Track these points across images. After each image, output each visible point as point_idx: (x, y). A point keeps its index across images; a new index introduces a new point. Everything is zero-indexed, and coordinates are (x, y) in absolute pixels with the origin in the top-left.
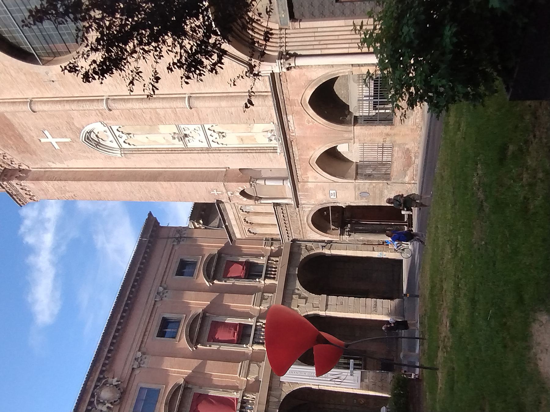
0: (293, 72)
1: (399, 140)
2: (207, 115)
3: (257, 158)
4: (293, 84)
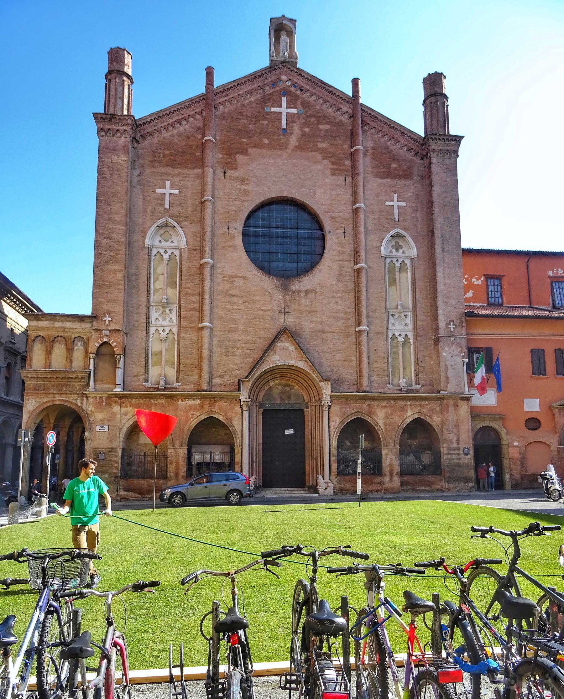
0: (238, 409)
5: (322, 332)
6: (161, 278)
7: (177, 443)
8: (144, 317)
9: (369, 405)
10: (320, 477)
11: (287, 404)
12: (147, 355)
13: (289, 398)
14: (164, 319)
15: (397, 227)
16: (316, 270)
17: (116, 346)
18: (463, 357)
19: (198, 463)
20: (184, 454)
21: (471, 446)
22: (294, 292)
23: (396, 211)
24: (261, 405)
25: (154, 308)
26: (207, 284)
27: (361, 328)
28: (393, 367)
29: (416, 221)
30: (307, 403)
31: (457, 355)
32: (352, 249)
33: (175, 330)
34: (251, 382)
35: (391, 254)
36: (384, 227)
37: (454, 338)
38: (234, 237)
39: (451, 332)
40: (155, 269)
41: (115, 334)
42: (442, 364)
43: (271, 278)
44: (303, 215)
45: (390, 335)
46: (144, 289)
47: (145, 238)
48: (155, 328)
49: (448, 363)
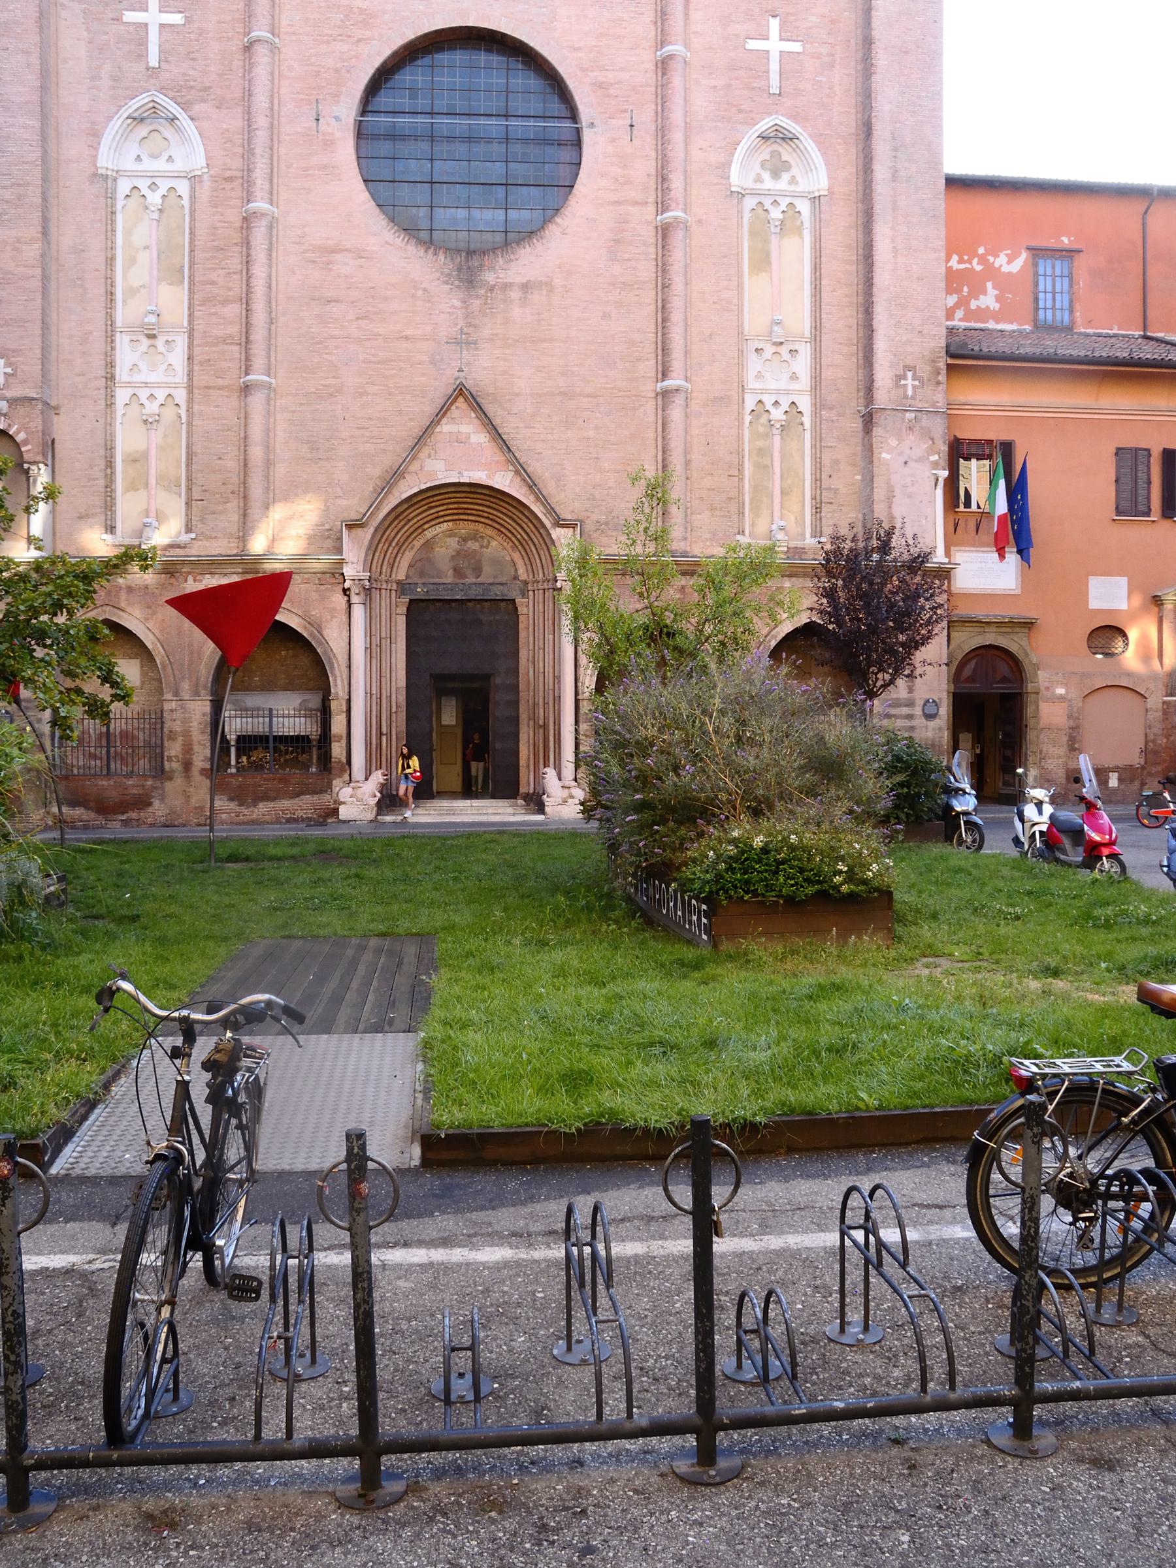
0: (340, 600)
1: (174, 787)
2: (217, 406)
3: (92, 486)
4: (314, 596)
5: (565, 394)
6: (144, 258)
7: (186, 685)
8: (98, 363)
9: (683, 587)
10: (551, 773)
11: (471, 586)
12: (110, 464)
13: (478, 570)
14: (153, 367)
15: (777, 113)
16: (552, 230)
17: (26, 442)
18: (935, 465)
19: (239, 736)
20: (204, 715)
21: (944, 695)
22: (492, 289)
23: (774, 67)
24: (403, 587)
25: (126, 338)
26: (259, 271)
27: (668, 383)
28: (755, 488)
29: (828, 96)
30: (526, 583)
31: (920, 460)
32: (653, 171)
33: (181, 395)
34: (371, 530)
35: (759, 186)
36: (740, 111)
37: (913, 415)
38: (333, 142)
39: (906, 397)
40: (128, 233)
41: (21, 410)
42: (879, 482)
43: (431, 251)
44: (525, 80)
45: (750, 403)
46: (97, 290)
47: (97, 149)
48: (130, 391)
49: (895, 478)
